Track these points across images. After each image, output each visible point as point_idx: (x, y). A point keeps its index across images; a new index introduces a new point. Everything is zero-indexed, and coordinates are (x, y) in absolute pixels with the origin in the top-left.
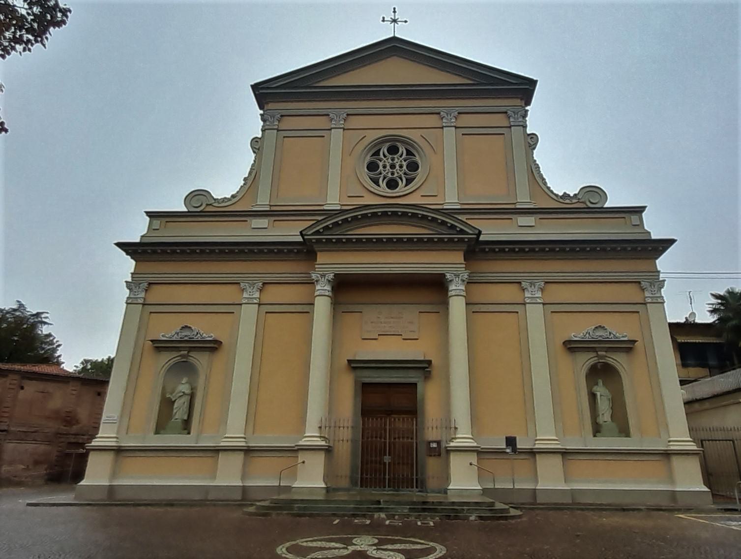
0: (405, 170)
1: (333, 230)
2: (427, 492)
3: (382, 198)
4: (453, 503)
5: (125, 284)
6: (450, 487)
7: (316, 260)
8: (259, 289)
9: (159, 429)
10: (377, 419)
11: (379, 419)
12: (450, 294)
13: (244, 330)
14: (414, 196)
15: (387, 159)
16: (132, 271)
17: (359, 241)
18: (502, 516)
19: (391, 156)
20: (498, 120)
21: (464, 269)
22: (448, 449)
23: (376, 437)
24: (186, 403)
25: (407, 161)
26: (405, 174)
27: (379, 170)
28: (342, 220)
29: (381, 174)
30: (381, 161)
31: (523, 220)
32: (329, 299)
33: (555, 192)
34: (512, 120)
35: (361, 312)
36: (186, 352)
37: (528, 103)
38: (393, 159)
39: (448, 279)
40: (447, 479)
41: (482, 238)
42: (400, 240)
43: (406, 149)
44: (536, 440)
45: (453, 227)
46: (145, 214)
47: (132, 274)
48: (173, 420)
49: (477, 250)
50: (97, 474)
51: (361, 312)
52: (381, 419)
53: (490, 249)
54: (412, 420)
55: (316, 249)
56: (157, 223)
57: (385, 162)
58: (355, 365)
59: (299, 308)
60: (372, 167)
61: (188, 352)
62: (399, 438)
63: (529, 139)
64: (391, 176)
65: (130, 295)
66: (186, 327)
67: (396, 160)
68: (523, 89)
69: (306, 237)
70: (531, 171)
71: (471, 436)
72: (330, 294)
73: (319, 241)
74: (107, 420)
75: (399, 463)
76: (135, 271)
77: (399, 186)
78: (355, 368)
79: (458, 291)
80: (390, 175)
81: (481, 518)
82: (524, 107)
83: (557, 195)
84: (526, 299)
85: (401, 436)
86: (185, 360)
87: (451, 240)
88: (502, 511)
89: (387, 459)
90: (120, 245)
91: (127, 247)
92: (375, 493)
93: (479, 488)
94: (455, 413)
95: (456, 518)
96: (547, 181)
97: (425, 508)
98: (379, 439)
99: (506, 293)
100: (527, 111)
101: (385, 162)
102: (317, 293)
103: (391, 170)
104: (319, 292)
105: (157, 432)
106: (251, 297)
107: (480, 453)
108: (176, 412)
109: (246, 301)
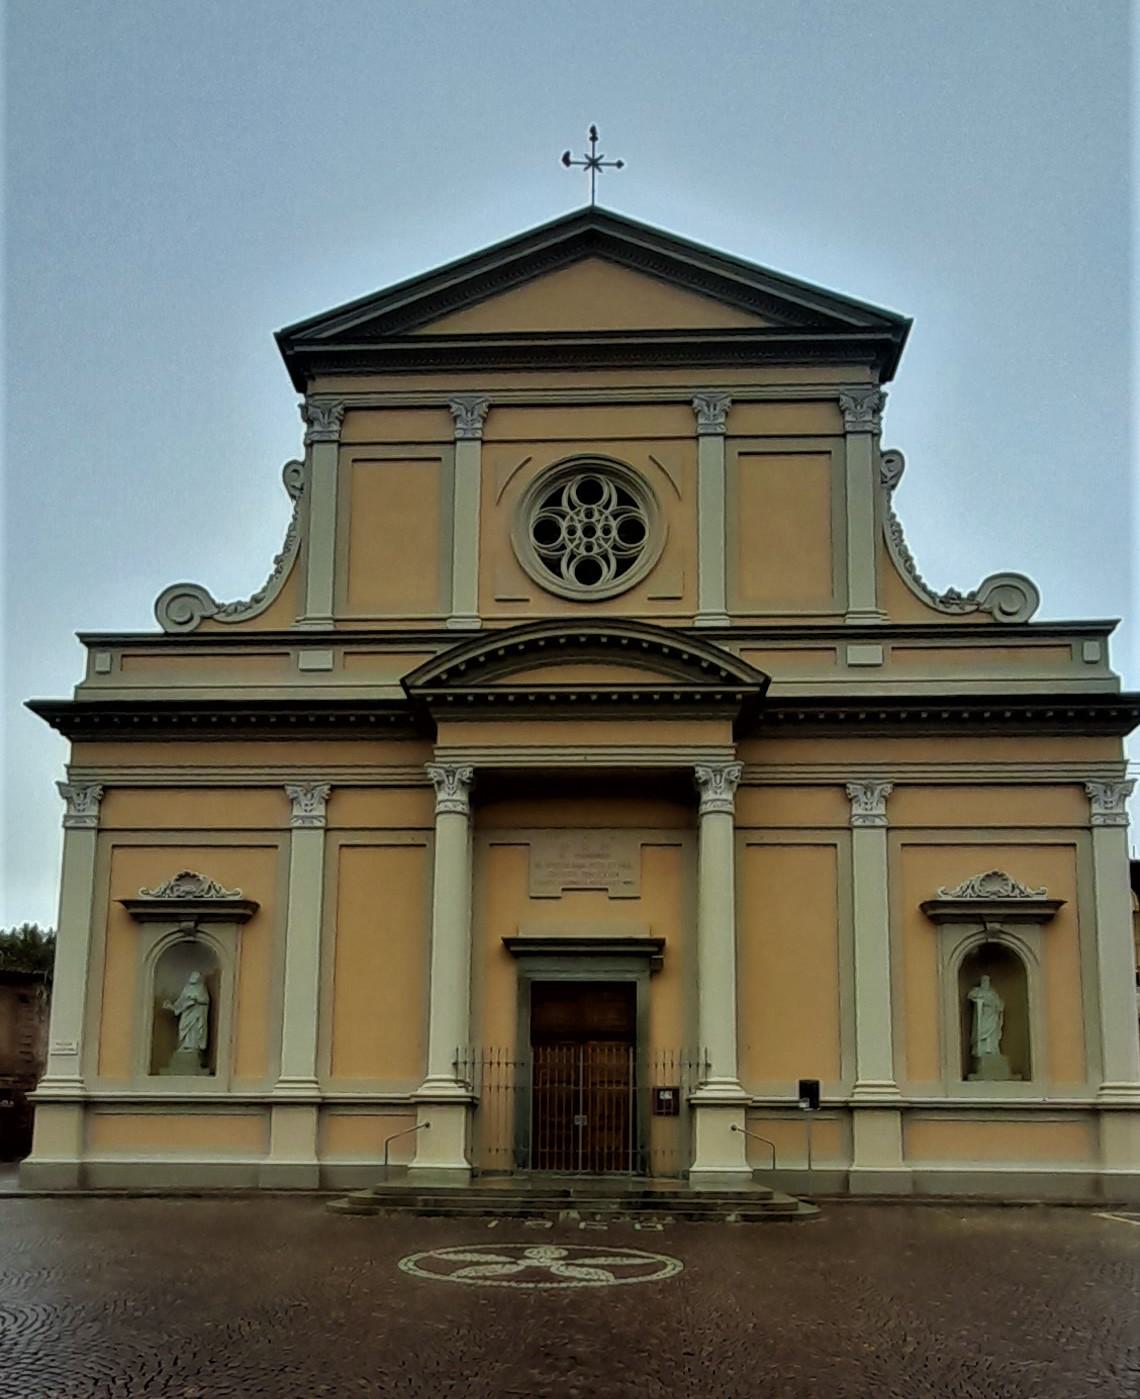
0: (615, 540)
1: (469, 677)
2: (652, 1177)
3: (568, 605)
4: (698, 1195)
5: (56, 788)
6: (694, 1169)
7: (435, 740)
8: (323, 798)
9: (156, 1067)
10: (561, 1049)
11: (565, 1050)
12: (704, 808)
13: (298, 881)
14: (636, 600)
15: (577, 514)
16: (67, 760)
17: (521, 699)
18: (785, 1216)
19: (586, 506)
20: (817, 419)
21: (732, 758)
22: (693, 1102)
23: (560, 1082)
24: (201, 1020)
25: (619, 519)
26: (615, 547)
27: (561, 538)
28: (485, 654)
29: (563, 547)
30: (563, 517)
31: (859, 652)
32: (465, 818)
33: (930, 587)
34: (848, 418)
35: (528, 844)
36: (192, 924)
37: (887, 375)
38: (589, 514)
39: (700, 778)
40: (691, 1155)
41: (771, 692)
42: (604, 698)
43: (618, 490)
44: (856, 1087)
45: (714, 669)
46: (77, 640)
47: (69, 767)
48: (180, 1050)
49: (761, 719)
50: (54, 1144)
51: (528, 844)
52: (569, 1049)
53: (787, 715)
54: (627, 1051)
55: (435, 716)
56: (104, 659)
57: (572, 519)
58: (517, 949)
59: (406, 838)
60: (546, 531)
61: (196, 926)
62: (602, 1082)
63: (884, 464)
64: (585, 553)
65: (68, 811)
66: (187, 874)
67: (596, 515)
68: (877, 341)
69: (412, 691)
70: (881, 542)
71: (735, 1080)
72: (466, 809)
73: (440, 700)
74: (58, 1050)
75: (602, 1129)
76: (72, 761)
77: (602, 578)
78: (516, 955)
79: (719, 803)
80: (583, 551)
81: (746, 1218)
82: (878, 386)
83: (932, 595)
84: (853, 819)
85: (606, 1079)
86: (191, 938)
87: (708, 698)
88: (784, 1207)
89: (580, 1120)
90: (38, 707)
91: (50, 712)
92: (553, 1179)
93: (748, 1169)
94: (707, 1037)
95: (702, 1217)
96: (915, 562)
97: (648, 1203)
98: (564, 1085)
99: (817, 807)
100: (883, 397)
101: (572, 519)
102: (440, 808)
103: (585, 540)
104: (442, 805)
105: (154, 1072)
106: (308, 814)
107: (751, 1109)
108: (185, 1037)
109: (298, 823)
